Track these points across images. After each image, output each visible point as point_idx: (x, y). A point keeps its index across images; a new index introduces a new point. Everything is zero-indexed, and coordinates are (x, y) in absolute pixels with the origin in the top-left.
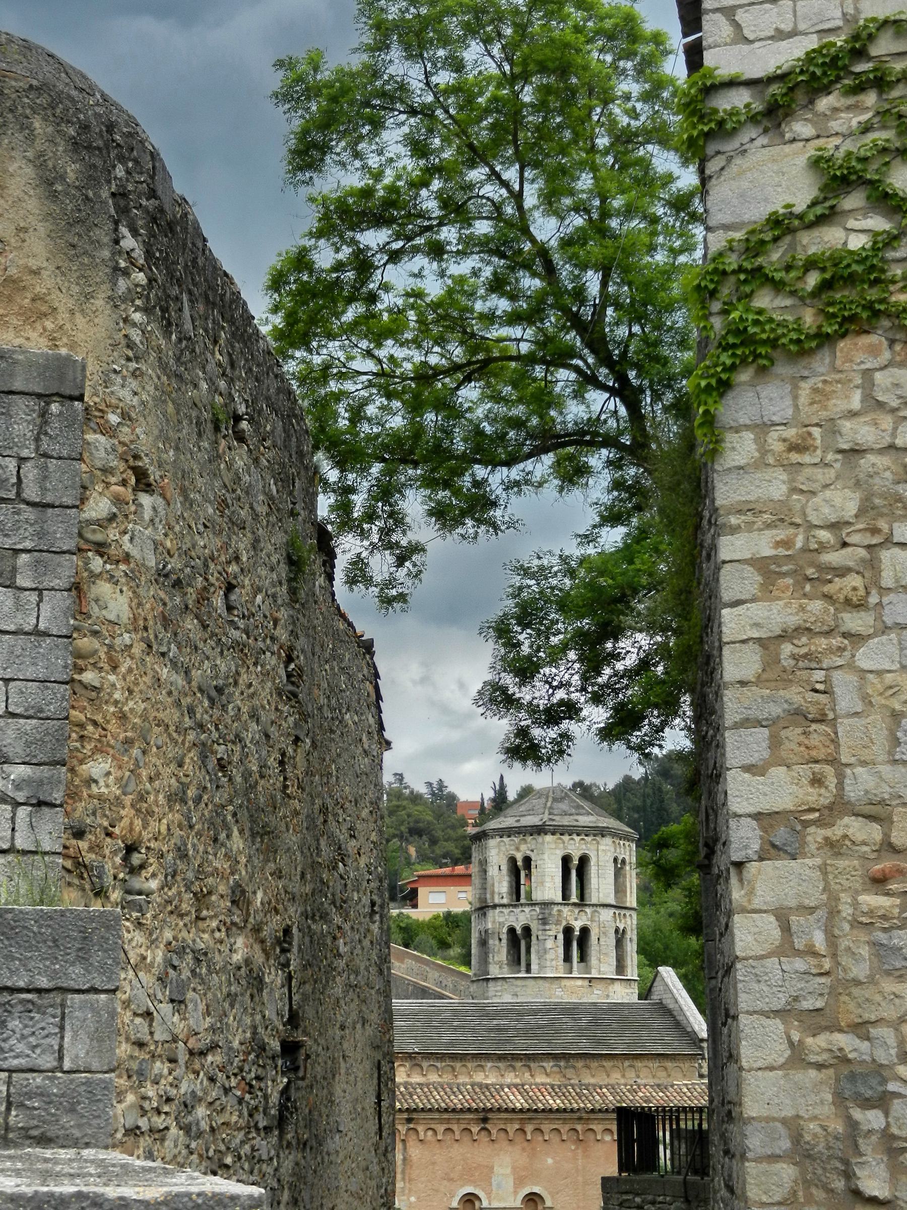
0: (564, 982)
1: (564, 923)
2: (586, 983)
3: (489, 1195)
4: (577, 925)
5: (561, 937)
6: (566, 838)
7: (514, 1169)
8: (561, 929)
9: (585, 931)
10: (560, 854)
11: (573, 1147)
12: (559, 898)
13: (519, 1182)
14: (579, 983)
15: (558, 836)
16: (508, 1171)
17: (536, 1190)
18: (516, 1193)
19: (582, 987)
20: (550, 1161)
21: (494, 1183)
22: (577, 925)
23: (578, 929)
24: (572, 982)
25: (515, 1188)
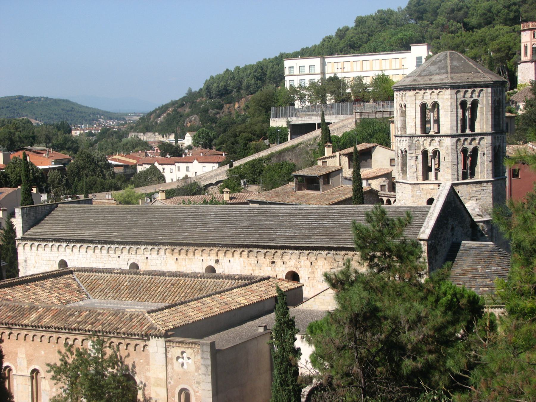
0: (422, 186)
1: (422, 148)
2: (436, 186)
3: (16, 367)
4: (430, 150)
5: (420, 157)
6: (422, 92)
7: (27, 355)
8: (420, 152)
9: (436, 153)
10: (418, 103)
11: (53, 346)
12: (419, 132)
13: (29, 362)
14: (432, 186)
15: (417, 91)
16: (24, 356)
17: (37, 367)
18: (28, 368)
19: (434, 189)
20: (43, 352)
21: (18, 362)
22: (430, 150)
23: (431, 152)
24: (427, 186)
25: (28, 365)
